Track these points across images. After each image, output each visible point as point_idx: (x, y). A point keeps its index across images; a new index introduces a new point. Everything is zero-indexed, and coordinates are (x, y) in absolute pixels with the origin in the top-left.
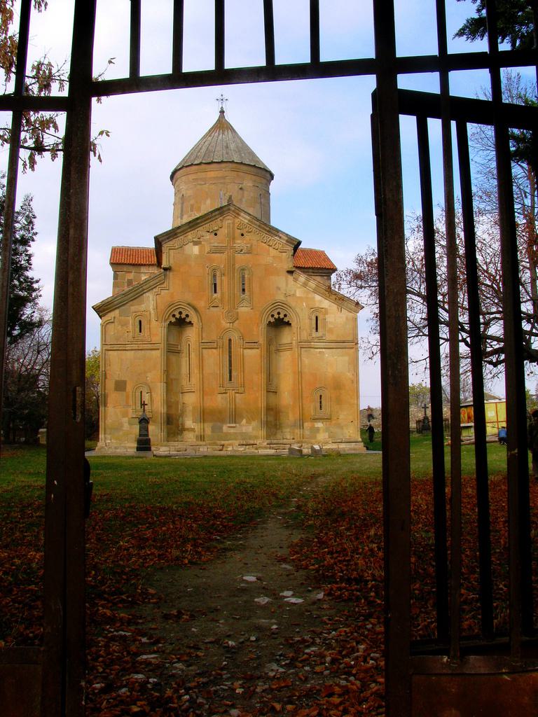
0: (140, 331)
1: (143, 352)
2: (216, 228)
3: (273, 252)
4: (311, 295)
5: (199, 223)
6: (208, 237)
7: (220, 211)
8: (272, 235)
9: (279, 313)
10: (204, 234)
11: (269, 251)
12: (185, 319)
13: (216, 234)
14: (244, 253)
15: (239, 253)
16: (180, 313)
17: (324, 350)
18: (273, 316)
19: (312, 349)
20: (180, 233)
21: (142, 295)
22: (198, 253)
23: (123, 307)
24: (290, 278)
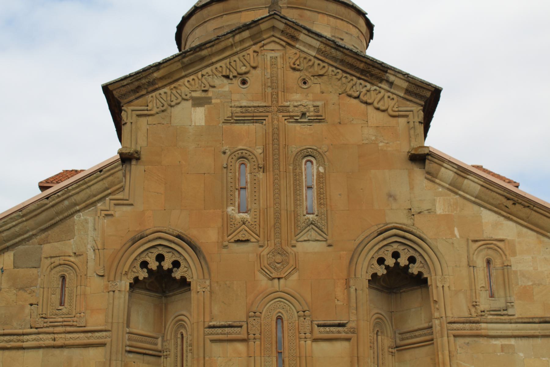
0: (62, 304)
1: (66, 352)
2: (244, 69)
3: (375, 117)
4: (472, 209)
5: (203, 59)
6: (227, 88)
7: (255, 30)
8: (375, 82)
9: (396, 255)
10: (218, 81)
11: (366, 115)
12: (170, 271)
13: (244, 82)
14: (311, 121)
15: (297, 121)
16: (160, 258)
17: (512, 341)
18: (381, 261)
19: (481, 340)
20: (162, 78)
21: (72, 214)
22: (203, 124)
23: (21, 247)
24: (418, 173)
